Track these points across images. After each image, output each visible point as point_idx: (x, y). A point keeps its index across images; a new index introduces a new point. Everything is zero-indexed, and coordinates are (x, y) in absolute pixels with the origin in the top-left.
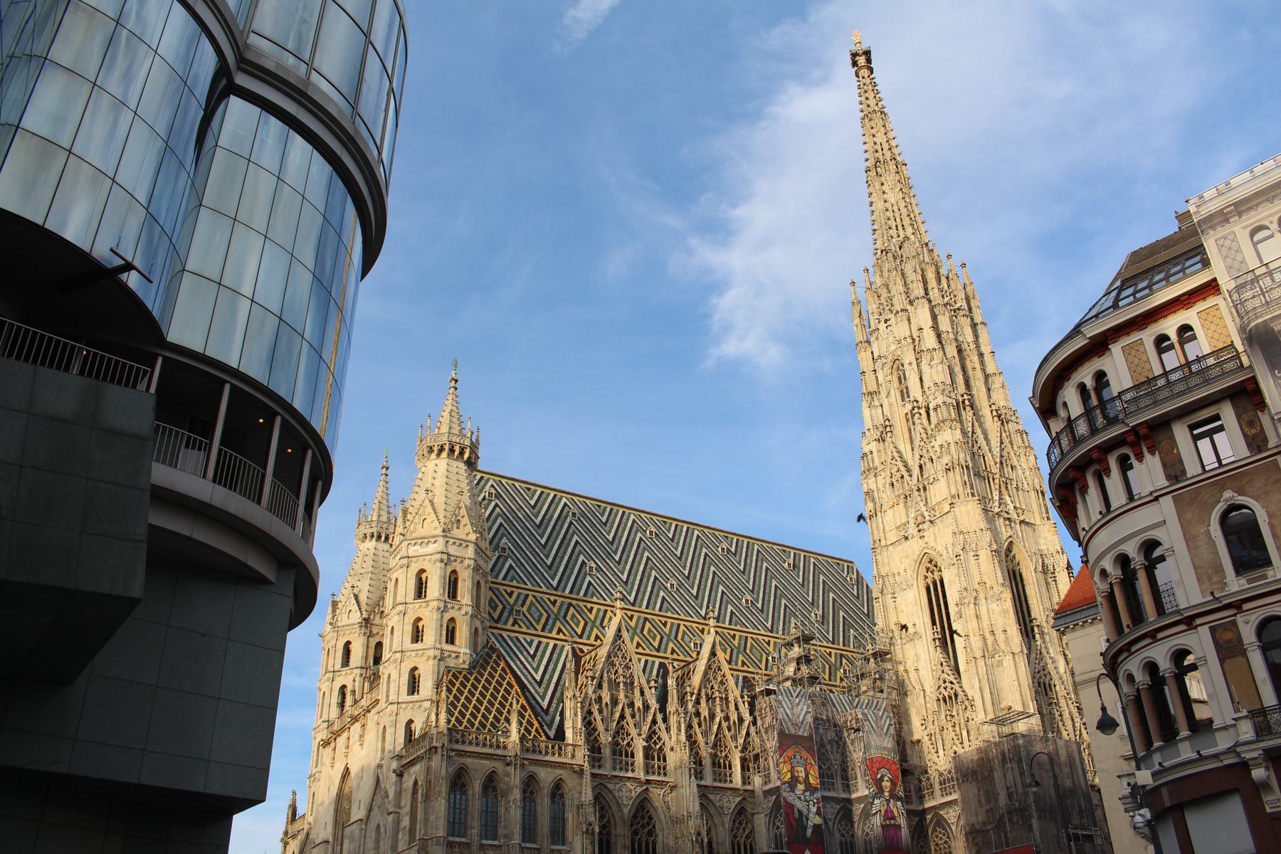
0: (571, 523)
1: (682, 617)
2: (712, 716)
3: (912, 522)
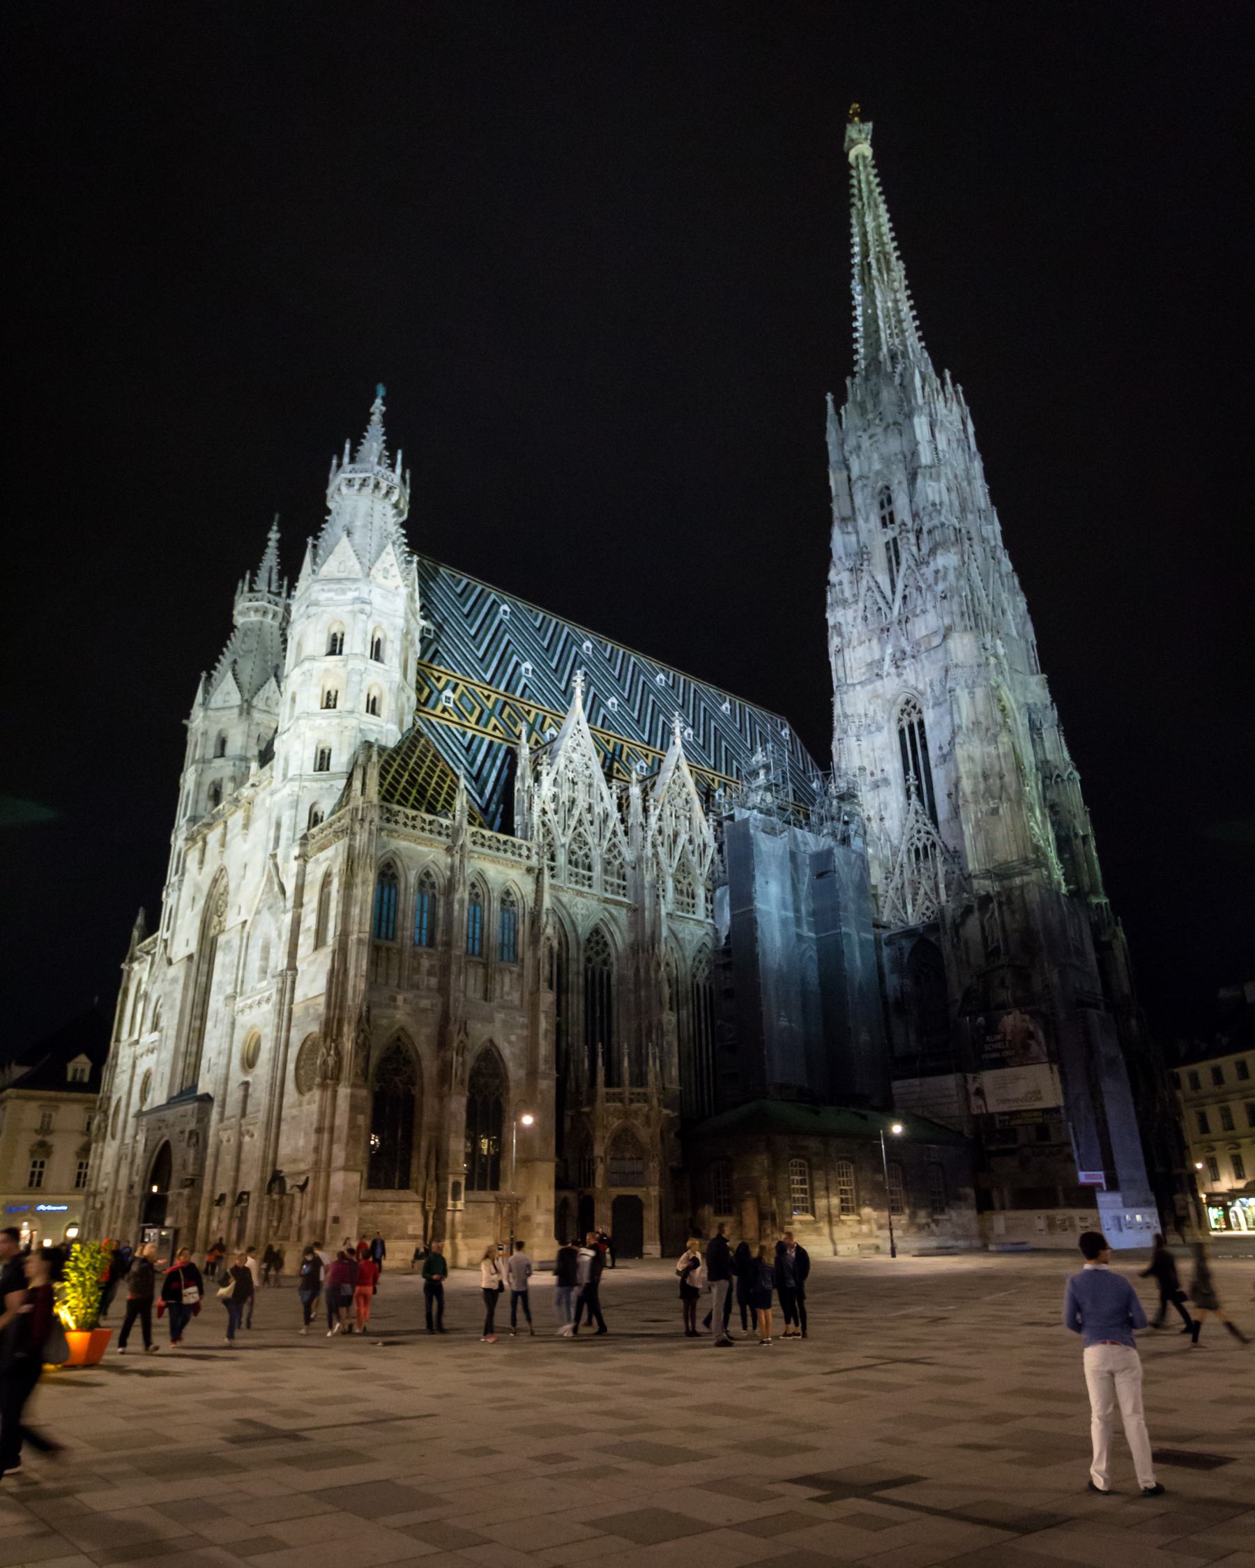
0: (501, 621)
1: (625, 738)
2: (676, 835)
3: (888, 659)
